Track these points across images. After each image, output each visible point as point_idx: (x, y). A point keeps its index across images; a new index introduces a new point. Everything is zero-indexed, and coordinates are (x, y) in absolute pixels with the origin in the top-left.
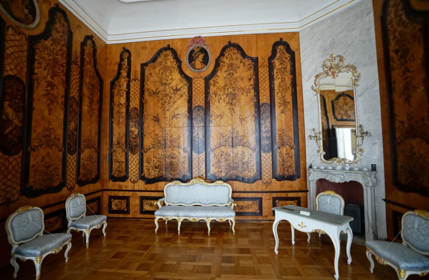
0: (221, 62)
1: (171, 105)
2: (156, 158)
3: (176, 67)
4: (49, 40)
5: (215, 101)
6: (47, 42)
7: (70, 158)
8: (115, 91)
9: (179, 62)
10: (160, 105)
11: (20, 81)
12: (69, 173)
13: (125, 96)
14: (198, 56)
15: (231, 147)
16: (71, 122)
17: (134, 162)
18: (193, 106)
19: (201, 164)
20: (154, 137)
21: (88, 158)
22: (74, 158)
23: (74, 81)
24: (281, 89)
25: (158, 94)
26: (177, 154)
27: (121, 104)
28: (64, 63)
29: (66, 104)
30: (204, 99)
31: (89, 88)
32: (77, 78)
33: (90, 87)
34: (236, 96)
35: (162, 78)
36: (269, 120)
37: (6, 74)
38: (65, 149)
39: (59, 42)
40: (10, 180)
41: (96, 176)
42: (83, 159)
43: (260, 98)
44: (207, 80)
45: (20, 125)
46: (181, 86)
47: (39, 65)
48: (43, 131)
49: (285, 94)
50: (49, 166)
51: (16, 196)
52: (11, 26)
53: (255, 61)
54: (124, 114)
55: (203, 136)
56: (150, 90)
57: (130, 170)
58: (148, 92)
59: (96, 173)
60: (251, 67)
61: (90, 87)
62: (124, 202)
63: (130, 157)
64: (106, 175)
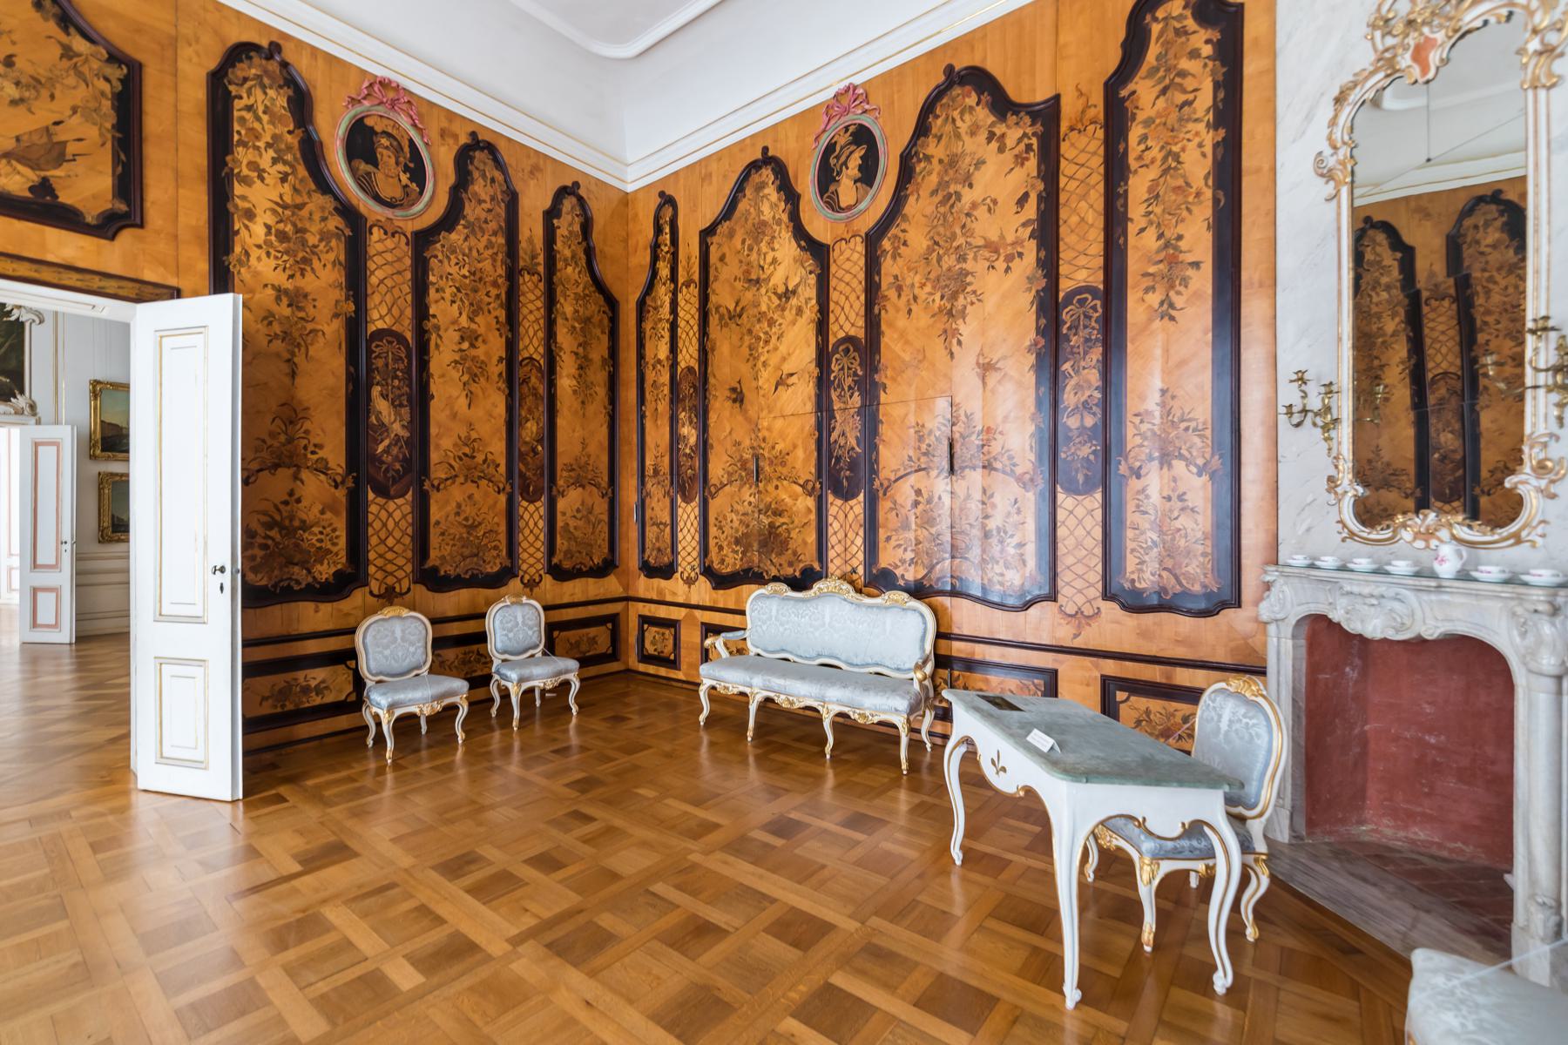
0: (920, 161)
2: (737, 512)
3: (785, 217)
4: (460, 227)
6: (453, 236)
7: (526, 509)
8: (648, 326)
9: (791, 197)
11: (400, 338)
12: (525, 545)
13: (667, 335)
14: (845, 164)
15: (946, 474)
16: (528, 420)
19: (851, 535)
21: (578, 511)
22: (537, 509)
23: (532, 318)
24: (1158, 210)
26: (788, 500)
27: (659, 361)
28: (500, 276)
31: (574, 328)
32: (538, 309)
33: (577, 325)
34: (969, 279)
36: (1096, 354)
37: (372, 328)
38: (512, 486)
39: (484, 226)
40: (391, 549)
41: (605, 561)
42: (564, 514)
43: (1063, 269)
44: (872, 241)
45: (406, 434)
47: (438, 296)
48: (455, 445)
49: (1180, 230)
51: (405, 584)
52: (377, 224)
53: (1047, 115)
54: (666, 390)
55: (857, 438)
57: (680, 548)
59: (606, 551)
60: (1029, 148)
61: (577, 325)
62: (668, 633)
63: (680, 511)
64: (631, 557)
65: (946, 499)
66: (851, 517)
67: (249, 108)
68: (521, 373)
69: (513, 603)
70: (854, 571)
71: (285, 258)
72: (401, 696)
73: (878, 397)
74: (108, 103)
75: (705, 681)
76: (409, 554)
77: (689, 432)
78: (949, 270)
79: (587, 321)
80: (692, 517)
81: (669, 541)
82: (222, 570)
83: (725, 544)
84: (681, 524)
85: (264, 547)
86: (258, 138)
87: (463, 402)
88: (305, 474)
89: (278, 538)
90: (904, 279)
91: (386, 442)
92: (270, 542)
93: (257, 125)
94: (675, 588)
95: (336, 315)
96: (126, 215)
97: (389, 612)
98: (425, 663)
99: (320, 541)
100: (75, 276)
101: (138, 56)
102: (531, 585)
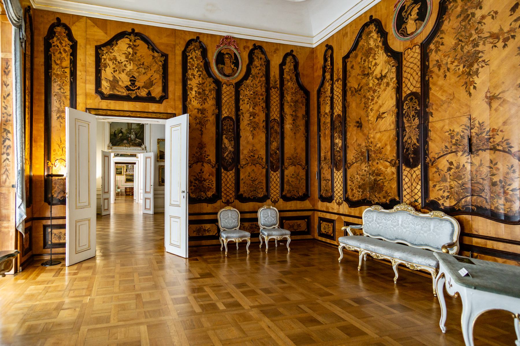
1: (374, 101)
4: (250, 78)
5: (438, 76)
6: (248, 81)
7: (273, 174)
8: (321, 100)
10: (362, 105)
12: (272, 187)
13: (329, 102)
16: (273, 142)
17: (339, 180)
18: (404, 95)
20: (357, 148)
21: (293, 175)
22: (277, 174)
23: (275, 104)
25: (360, 90)
27: (326, 114)
28: (264, 91)
29: (267, 127)
30: (419, 80)
31: (291, 105)
32: (277, 101)
33: (292, 104)
35: (364, 67)
37: (223, 117)
38: (268, 166)
39: (258, 75)
40: (228, 188)
41: (304, 194)
42: (287, 176)
46: (387, 71)
47: (243, 102)
48: (248, 152)
50: (254, 181)
51: (233, 199)
52: (225, 83)
54: (329, 125)
56: (352, 89)
57: (335, 190)
58: (350, 92)
59: (305, 190)
61: (292, 104)
63: (335, 174)
65: (468, 167)
66: (414, 176)
67: (191, 58)
68: (271, 125)
69: (267, 208)
70: (416, 201)
71: (200, 99)
72: (229, 235)
73: (428, 119)
74: (161, 68)
75: (341, 244)
76: (234, 189)
77: (339, 142)
78: (468, 52)
79: (296, 102)
80: (340, 177)
81: (330, 187)
82: (184, 192)
83: (354, 188)
84: (336, 180)
85: (194, 186)
86: (193, 66)
87: (251, 137)
88: (205, 164)
89: (198, 183)
90: (442, 61)
91: (227, 153)
92: (196, 185)
93: (193, 63)
94: (333, 206)
95: (213, 114)
96: (165, 96)
97: (228, 208)
98: (238, 226)
99: (209, 185)
100: (155, 114)
101: (167, 53)
102: (275, 202)
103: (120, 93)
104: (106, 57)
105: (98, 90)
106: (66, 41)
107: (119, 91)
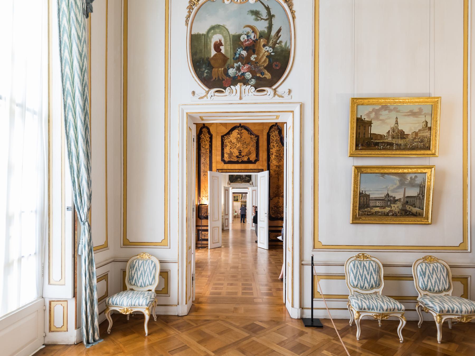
67: (272, 136)
71: (277, 160)
74: (255, 144)
85: (274, 210)
86: (274, 141)
89: (276, 209)
92: (275, 210)
93: (274, 139)
96: (257, 159)
100: (251, 170)
101: (258, 135)
103: (233, 160)
104: (226, 141)
105: (223, 160)
106: (208, 135)
107: (233, 159)
